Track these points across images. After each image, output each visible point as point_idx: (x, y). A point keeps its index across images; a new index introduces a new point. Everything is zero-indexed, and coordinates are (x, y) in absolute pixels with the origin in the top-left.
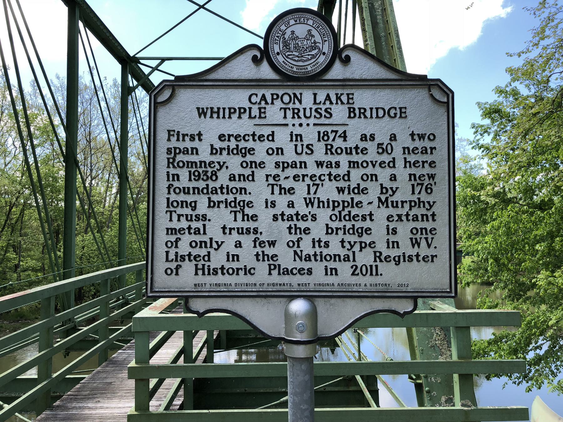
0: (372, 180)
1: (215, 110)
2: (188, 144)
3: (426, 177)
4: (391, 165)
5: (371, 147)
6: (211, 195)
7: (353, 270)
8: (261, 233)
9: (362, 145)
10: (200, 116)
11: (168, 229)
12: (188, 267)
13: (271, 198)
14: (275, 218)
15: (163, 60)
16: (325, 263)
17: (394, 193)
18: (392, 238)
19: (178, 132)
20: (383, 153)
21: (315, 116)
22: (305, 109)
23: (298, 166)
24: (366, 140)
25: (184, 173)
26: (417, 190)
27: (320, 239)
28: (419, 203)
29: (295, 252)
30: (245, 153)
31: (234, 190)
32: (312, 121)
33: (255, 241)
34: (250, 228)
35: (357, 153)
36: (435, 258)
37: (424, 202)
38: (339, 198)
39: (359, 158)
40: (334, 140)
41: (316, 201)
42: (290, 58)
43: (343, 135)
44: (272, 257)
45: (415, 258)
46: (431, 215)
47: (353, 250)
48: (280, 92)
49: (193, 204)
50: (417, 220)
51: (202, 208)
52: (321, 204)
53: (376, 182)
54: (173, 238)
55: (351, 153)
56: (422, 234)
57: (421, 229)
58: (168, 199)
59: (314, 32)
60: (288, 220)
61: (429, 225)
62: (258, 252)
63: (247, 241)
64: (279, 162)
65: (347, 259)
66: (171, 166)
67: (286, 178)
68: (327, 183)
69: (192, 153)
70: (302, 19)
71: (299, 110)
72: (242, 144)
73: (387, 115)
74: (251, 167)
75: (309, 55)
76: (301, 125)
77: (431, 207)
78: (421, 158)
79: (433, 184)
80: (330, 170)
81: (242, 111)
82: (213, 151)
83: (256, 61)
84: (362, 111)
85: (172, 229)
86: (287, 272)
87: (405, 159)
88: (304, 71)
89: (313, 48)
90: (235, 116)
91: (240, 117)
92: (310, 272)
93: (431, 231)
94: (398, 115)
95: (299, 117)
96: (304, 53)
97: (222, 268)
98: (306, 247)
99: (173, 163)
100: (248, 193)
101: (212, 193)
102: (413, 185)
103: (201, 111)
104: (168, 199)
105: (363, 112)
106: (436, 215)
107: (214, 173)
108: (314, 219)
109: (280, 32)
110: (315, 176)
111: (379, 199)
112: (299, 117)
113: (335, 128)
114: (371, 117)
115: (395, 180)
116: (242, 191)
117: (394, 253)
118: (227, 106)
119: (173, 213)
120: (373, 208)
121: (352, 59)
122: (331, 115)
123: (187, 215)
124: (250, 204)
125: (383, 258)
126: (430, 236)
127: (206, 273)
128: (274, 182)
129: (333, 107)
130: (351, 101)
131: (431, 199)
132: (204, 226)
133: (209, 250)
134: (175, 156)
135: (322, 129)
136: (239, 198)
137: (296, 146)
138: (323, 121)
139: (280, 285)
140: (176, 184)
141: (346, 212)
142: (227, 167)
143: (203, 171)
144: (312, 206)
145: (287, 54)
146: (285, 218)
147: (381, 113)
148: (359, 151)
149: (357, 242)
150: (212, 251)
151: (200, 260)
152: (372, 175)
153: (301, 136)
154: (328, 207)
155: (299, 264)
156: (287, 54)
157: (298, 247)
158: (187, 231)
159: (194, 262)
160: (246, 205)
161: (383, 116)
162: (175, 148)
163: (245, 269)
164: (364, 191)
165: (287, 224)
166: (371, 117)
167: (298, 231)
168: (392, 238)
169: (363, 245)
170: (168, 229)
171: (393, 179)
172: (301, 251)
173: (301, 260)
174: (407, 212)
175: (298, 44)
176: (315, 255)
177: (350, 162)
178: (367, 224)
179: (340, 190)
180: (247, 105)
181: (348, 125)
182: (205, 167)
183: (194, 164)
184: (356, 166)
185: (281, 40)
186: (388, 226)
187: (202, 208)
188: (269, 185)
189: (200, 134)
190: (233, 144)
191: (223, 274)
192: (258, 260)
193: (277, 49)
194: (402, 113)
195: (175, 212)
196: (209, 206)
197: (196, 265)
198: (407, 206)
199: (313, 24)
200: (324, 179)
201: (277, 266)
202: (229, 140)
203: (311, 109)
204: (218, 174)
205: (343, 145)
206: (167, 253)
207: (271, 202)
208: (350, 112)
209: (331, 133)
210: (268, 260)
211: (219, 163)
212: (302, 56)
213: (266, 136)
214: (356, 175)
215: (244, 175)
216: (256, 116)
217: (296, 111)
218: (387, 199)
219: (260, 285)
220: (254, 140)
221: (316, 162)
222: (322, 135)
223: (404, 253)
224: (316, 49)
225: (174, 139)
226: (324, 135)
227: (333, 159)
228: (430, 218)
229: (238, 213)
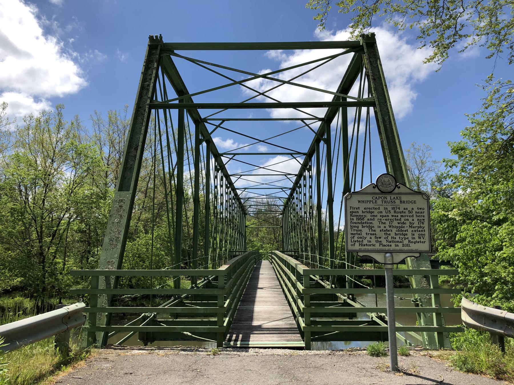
2: (356, 210)
5: (407, 211)
9: (404, 211)
12: (357, 244)
14: (381, 231)
15: (224, 120)
16: (395, 243)
18: (413, 236)
25: (355, 218)
26: (420, 223)
32: (390, 204)
39: (404, 214)
48: (381, 196)
59: (390, 180)
61: (423, 233)
65: (401, 242)
72: (371, 210)
78: (420, 214)
83: (374, 187)
86: (384, 246)
92: (391, 246)
97: (367, 244)
98: (390, 239)
105: (404, 202)
116: (371, 223)
117: (414, 240)
120: (408, 228)
135: (393, 206)
136: (371, 225)
138: (393, 204)
140: (353, 221)
147: (409, 202)
155: (388, 244)
164: (405, 223)
165: (384, 232)
168: (413, 236)
178: (406, 233)
179: (399, 223)
180: (372, 200)
189: (359, 208)
190: (368, 210)
194: (415, 202)
198: (417, 228)
214: (403, 219)
225: (352, 209)
227: (396, 215)
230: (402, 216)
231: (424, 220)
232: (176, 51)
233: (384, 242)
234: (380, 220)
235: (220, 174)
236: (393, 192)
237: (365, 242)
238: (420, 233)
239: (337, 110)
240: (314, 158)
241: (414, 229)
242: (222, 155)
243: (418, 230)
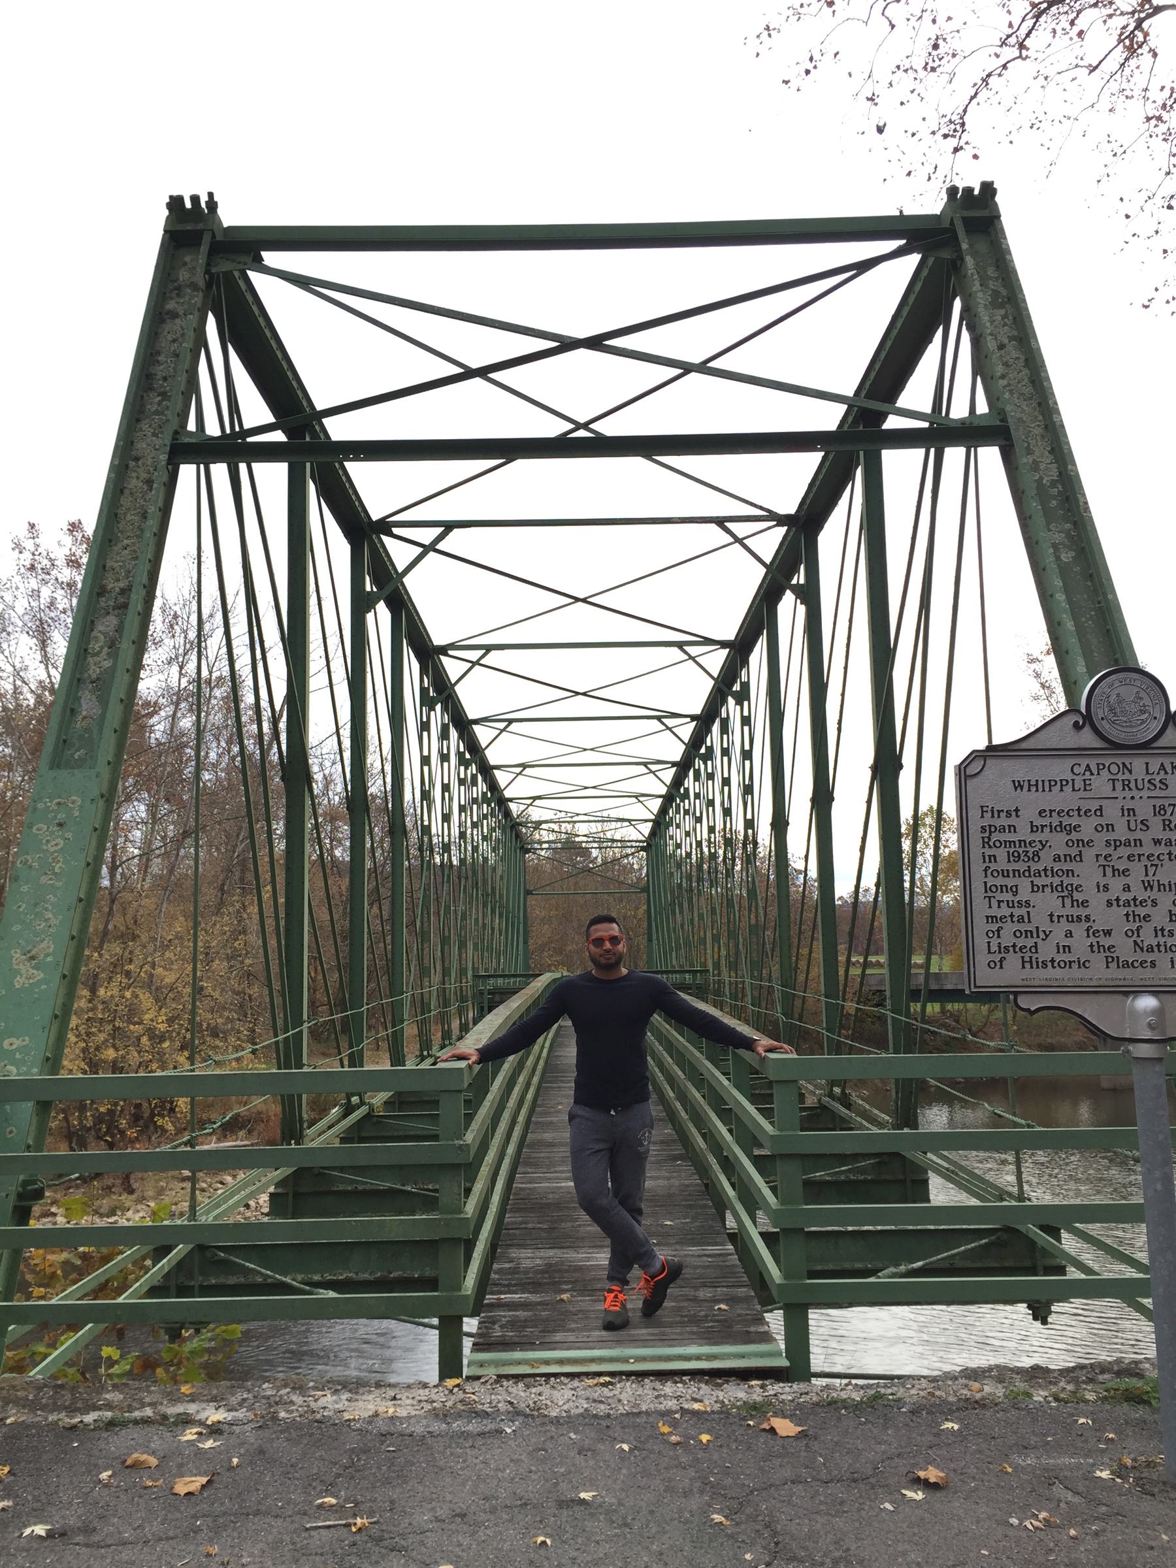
2: (1003, 821)
10: (1016, 788)
11: (987, 917)
12: (1013, 960)
14: (1109, 903)
15: (449, 526)
22: (1136, 780)
23: (1133, 844)
25: (1001, 854)
29: (1135, 941)
30: (1070, 831)
32: (1145, 793)
40: (1171, 814)
41: (1156, 883)
49: (1014, 889)
51: (1024, 894)
52: (1162, 887)
54: (994, 927)
58: (985, 883)
59: (1142, 694)
63: (1079, 930)
66: (986, 845)
71: (1129, 781)
81: (1064, 783)
82: (1034, 828)
83: (1076, 726)
86: (1127, 965)
89: (1143, 712)
95: (1130, 789)
97: (1053, 961)
99: (988, 843)
104: (985, 883)
110: (1153, 855)
112: (1130, 789)
122: (1167, 786)
123: (1008, 901)
127: (1035, 966)
129: (1168, 777)
132: (1028, 912)
134: (990, 835)
135: (1158, 803)
137: (1128, 821)
138: (1157, 793)
140: (993, 866)
146: (1121, 903)
150: (1039, 941)
153: (1133, 810)
154: (1170, 890)
155: (1141, 956)
157: (1138, 936)
158: (1009, 919)
162: (990, 826)
176: (1158, 945)
180: (1069, 777)
182: (1025, 846)
187: (1024, 894)
189: (1017, 810)
191: (1054, 967)
192: (1093, 952)
196: (1033, 891)
197: (1023, 957)
202: (1051, 816)
210: (1104, 951)
217: (1126, 783)
220: (1079, 815)
221: (1154, 839)
222: (1157, 809)
226: (1160, 809)
232: (271, 258)
233: (1124, 949)
234: (1105, 863)
235: (437, 717)
236: (1153, 745)
237: (1047, 951)
239: (849, 477)
240: (758, 656)
242: (444, 650)
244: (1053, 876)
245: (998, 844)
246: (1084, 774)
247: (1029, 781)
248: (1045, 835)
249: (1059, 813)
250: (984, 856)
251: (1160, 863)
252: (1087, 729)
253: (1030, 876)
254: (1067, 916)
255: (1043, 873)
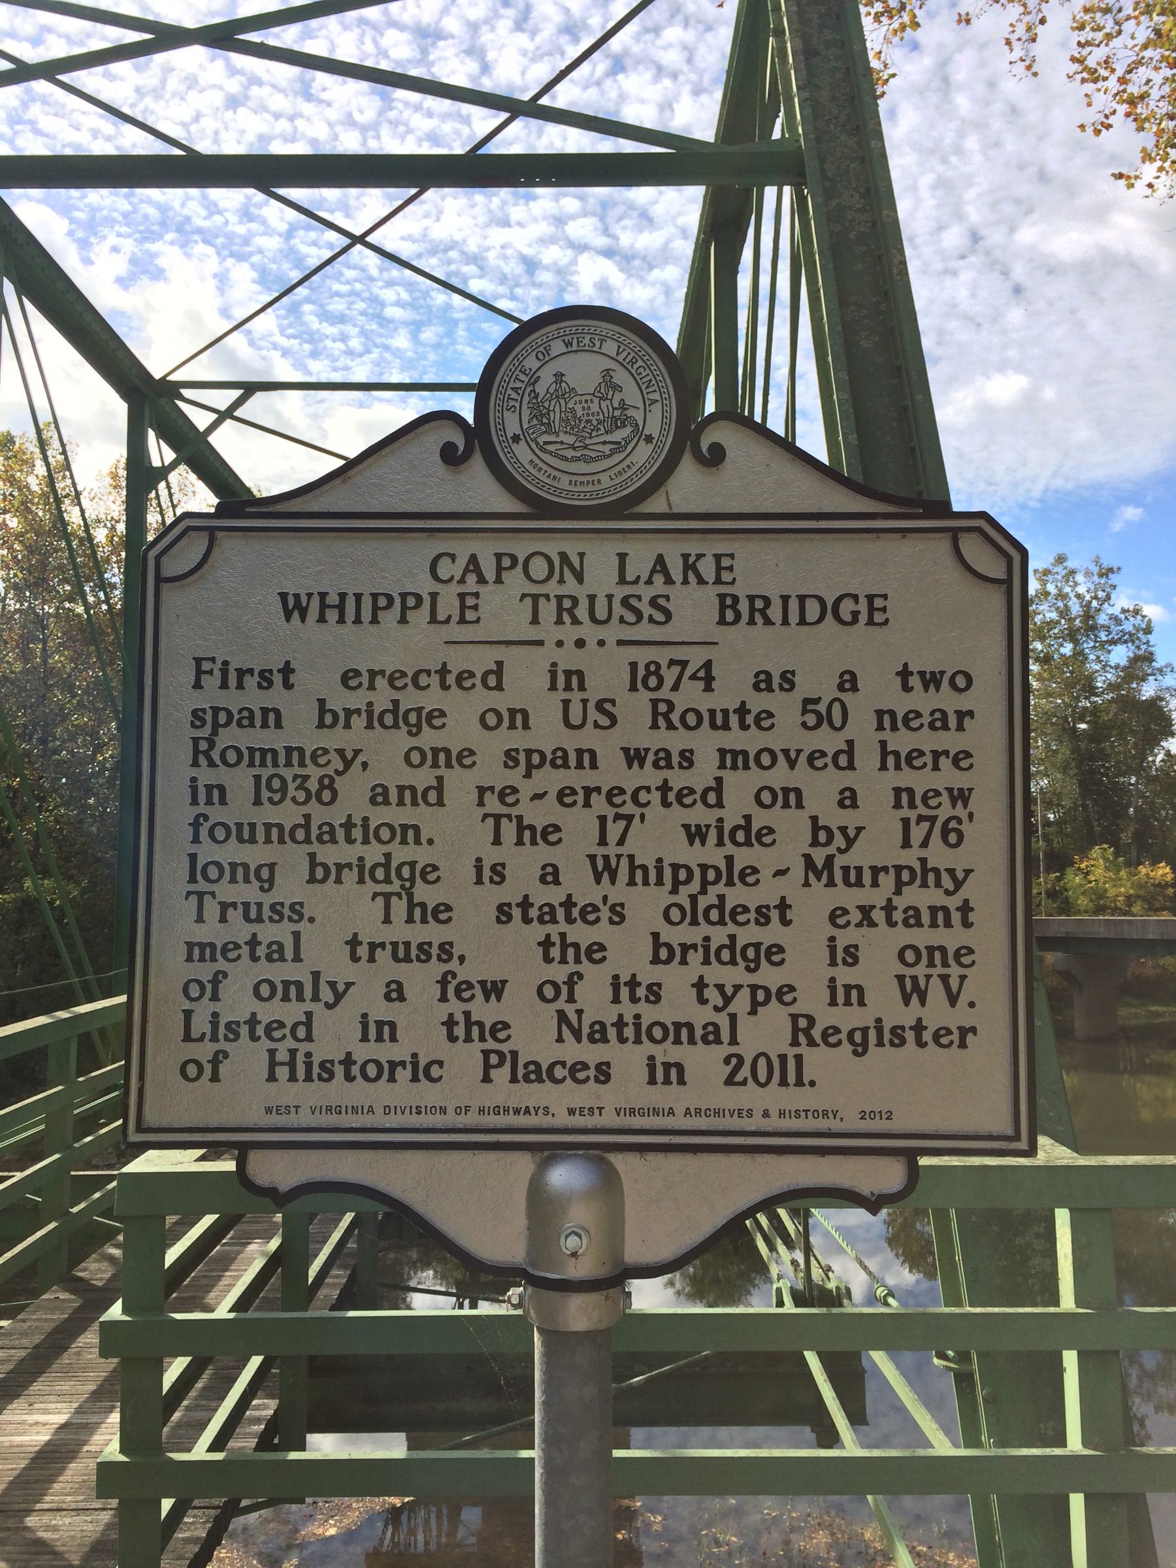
0: (786, 805)
1: (333, 599)
2: (253, 698)
3: (945, 798)
4: (843, 760)
6: (315, 847)
7: (729, 1069)
8: (462, 959)
9: (758, 701)
10: (288, 616)
11: (190, 946)
13: (491, 856)
14: (503, 913)
15: (250, 389)
16: (648, 1048)
17: (850, 842)
18: (845, 975)
19: (225, 663)
20: (818, 725)
21: (622, 617)
22: (592, 598)
24: (770, 689)
25: (239, 781)
26: (918, 832)
27: (634, 976)
28: (925, 873)
29: (562, 1017)
30: (419, 725)
31: (385, 834)
32: (613, 632)
33: (443, 982)
34: (430, 944)
35: (744, 727)
36: (970, 1036)
37: (936, 871)
38: (693, 856)
39: (750, 741)
40: (675, 687)
41: (624, 862)
42: (551, 453)
43: (702, 674)
44: (494, 1031)
45: (910, 1036)
46: (958, 909)
47: (731, 1009)
48: (521, 548)
49: (265, 874)
50: (919, 924)
52: (639, 874)
53: (799, 811)
54: (205, 972)
55: (726, 727)
56: (931, 964)
57: (931, 949)
58: (193, 858)
60: (541, 921)
61: (952, 938)
62: (451, 1015)
64: (517, 751)
65: (712, 1035)
66: (202, 760)
67: (538, 797)
68: (655, 809)
69: (265, 725)
70: (588, 337)
71: (575, 601)
72: (410, 699)
73: (829, 615)
74: (435, 765)
75: (604, 443)
76: (580, 643)
77: (958, 884)
78: (928, 741)
79: (965, 819)
80: (665, 773)
81: (411, 602)
82: (325, 716)
83: (451, 456)
84: (759, 604)
85: (202, 946)
86: (537, 1073)
87: (883, 744)
88: (590, 488)
89: (617, 423)
90: (390, 618)
91: (403, 620)
92: (603, 1073)
93: (957, 955)
94: (864, 617)
95: (576, 621)
96: (591, 438)
97: (348, 1061)
99: (207, 754)
100: (424, 840)
101: (320, 839)
102: (906, 822)
103: (291, 604)
104: (193, 858)
106: (972, 909)
107: (326, 781)
108: (616, 919)
109: (522, 377)
110: (622, 791)
111: (808, 858)
112: (576, 621)
113: (679, 653)
114: (785, 622)
115: (854, 805)
116: (409, 833)
117: (847, 1018)
118: (366, 590)
119: (207, 898)
121: (730, 454)
122: (668, 615)
123: (246, 905)
124: (429, 873)
125: (816, 1033)
126: (954, 971)
128: (504, 810)
129: (676, 591)
130: (726, 576)
131: (954, 859)
132: (297, 935)
133: (308, 1006)
134: (215, 732)
135: (643, 656)
136: (401, 854)
137: (566, 703)
138: (644, 631)
139: (517, 1111)
140: (217, 814)
141: (711, 898)
142: (365, 765)
143: (296, 777)
144: (613, 882)
145: (541, 440)
146: (533, 913)
148: (750, 719)
149: (742, 986)
150: (317, 1008)
151: (284, 1036)
152: (786, 791)
153: (580, 674)
154: (660, 882)
155: (572, 1051)
156: (541, 440)
157: (571, 999)
158: (245, 950)
159: (266, 1044)
160: (418, 875)
161: (821, 619)
162: (216, 710)
163: (415, 1065)
164: (762, 837)
165: (538, 932)
166: (785, 622)
167: (571, 952)
168: (845, 975)
169: (761, 995)
170: (190, 946)
171: (848, 802)
172: (580, 1012)
173: (579, 1040)
174: (890, 900)
175: (573, 410)
176: (620, 1024)
177: (722, 752)
178: (772, 933)
179: (695, 834)
180: (425, 586)
181: (716, 644)
183: (269, 756)
184: (740, 763)
185: (526, 399)
186: (832, 939)
188: (486, 816)
190: (382, 696)
191: (349, 1078)
192: (452, 1038)
193: (512, 428)
195: (213, 894)
196: (312, 880)
197: (272, 1053)
198: (887, 881)
199: (618, 354)
200: (649, 802)
201: (509, 1057)
202: (372, 687)
203: (610, 597)
204: (339, 783)
205: (704, 703)
206: (188, 1014)
207: (493, 868)
208: (723, 608)
209: (669, 667)
210: (482, 1039)
211: (341, 752)
212: (585, 447)
213: (479, 676)
215: (413, 789)
216: (450, 617)
217: (567, 604)
218: (830, 859)
219: (458, 1111)
220: (445, 687)
221: (626, 750)
222: (641, 673)
223: (879, 1020)
224: (625, 426)
225: (212, 682)
226: (648, 673)
227: (676, 741)
228: (956, 917)
229: (394, 899)
230: (732, 758)
231: (961, 796)
238: (923, 937)
241: (851, 898)
243: (900, 902)
244: (366, 841)
245: (232, 757)
246: (462, 581)
247: (323, 595)
248: (356, 735)
249: (391, 681)
250: (194, 790)
251: (637, 811)
252: (478, 464)
253: (308, 840)
254: (395, 945)
255: (340, 834)
